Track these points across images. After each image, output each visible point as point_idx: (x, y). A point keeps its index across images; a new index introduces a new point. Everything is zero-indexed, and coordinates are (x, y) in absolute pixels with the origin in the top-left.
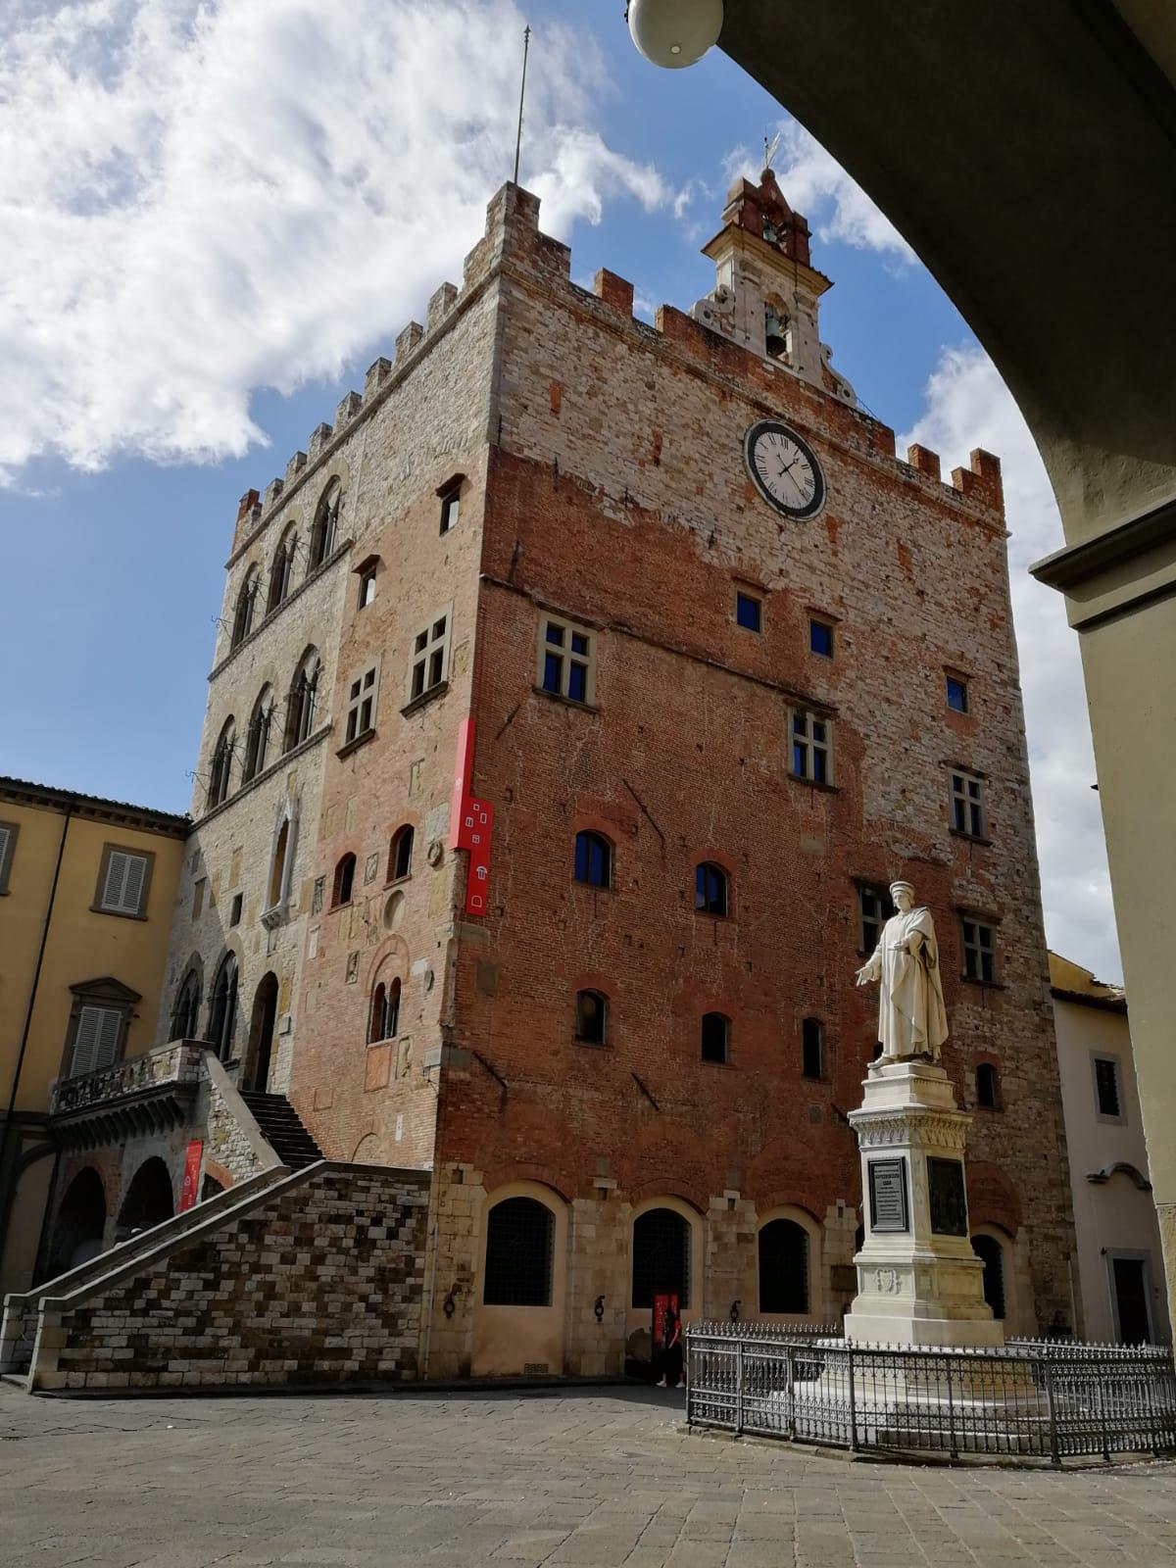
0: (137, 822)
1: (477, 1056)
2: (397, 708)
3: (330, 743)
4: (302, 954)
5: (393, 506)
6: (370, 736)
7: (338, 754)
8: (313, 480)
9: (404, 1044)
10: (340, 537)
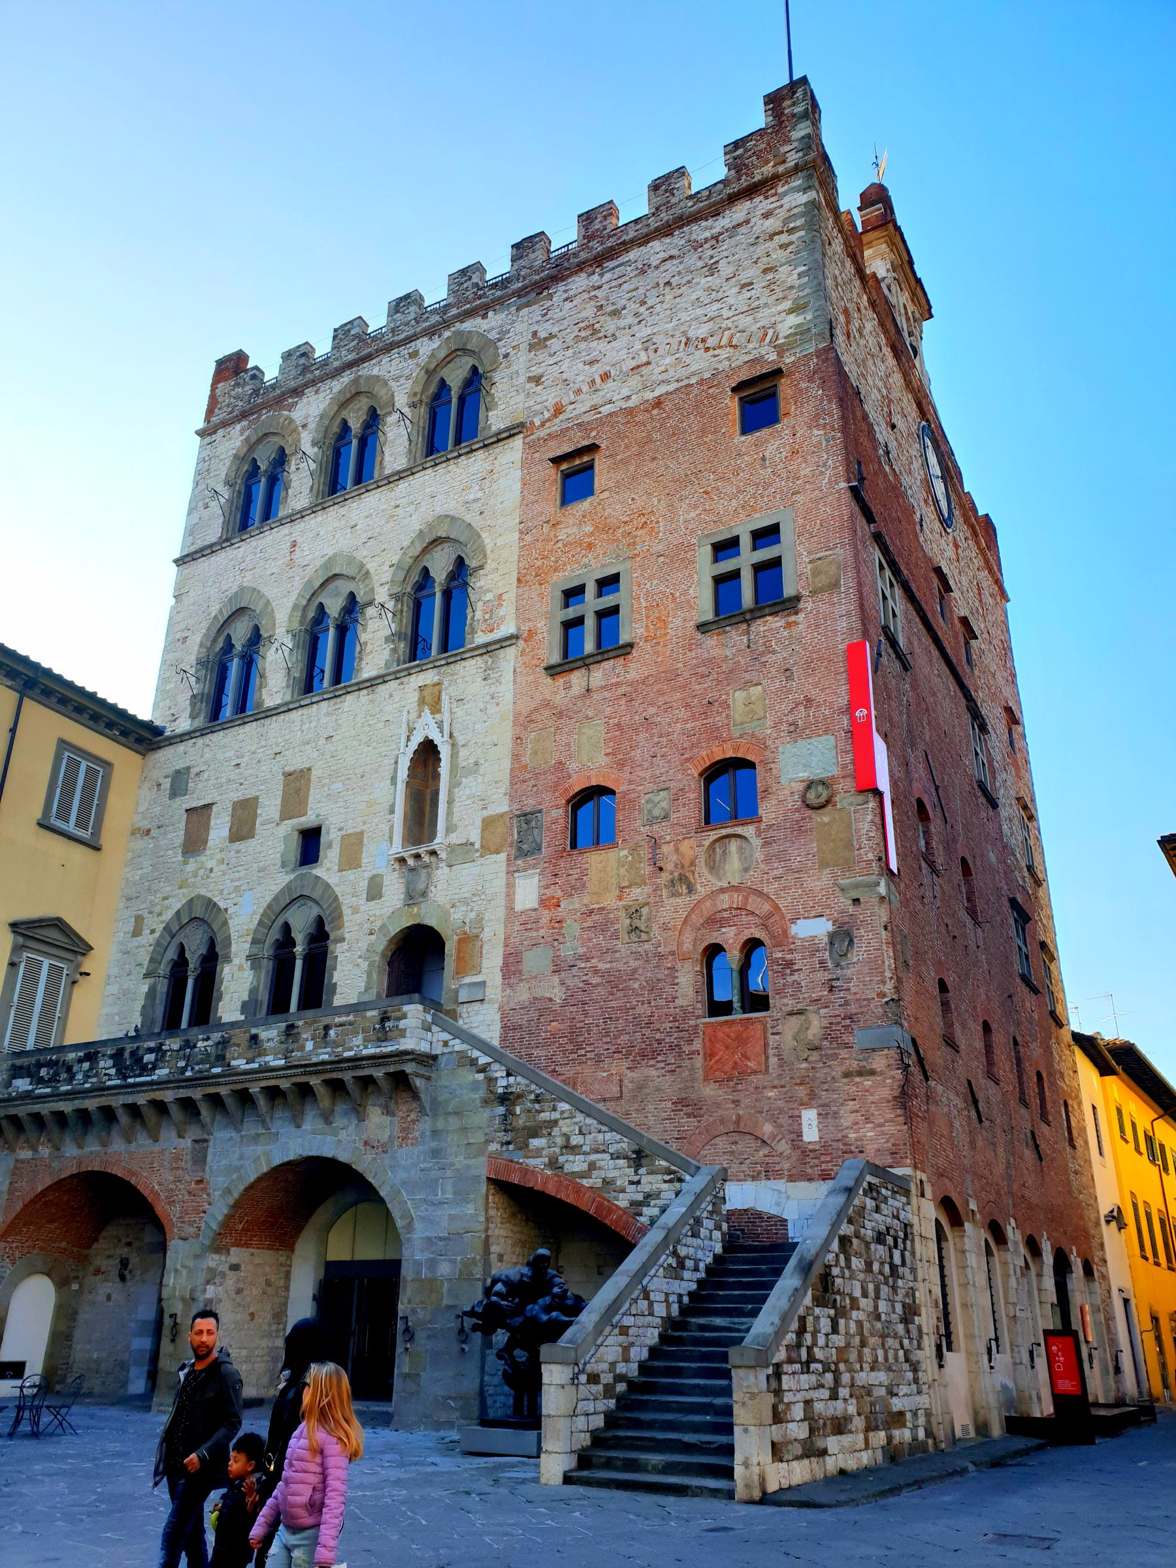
0: (95, 717)
1: (914, 1041)
2: (680, 624)
3: (523, 653)
4: (501, 901)
5: (621, 393)
6: (612, 647)
7: (546, 669)
8: (404, 351)
9: (795, 1022)
10: (496, 419)
